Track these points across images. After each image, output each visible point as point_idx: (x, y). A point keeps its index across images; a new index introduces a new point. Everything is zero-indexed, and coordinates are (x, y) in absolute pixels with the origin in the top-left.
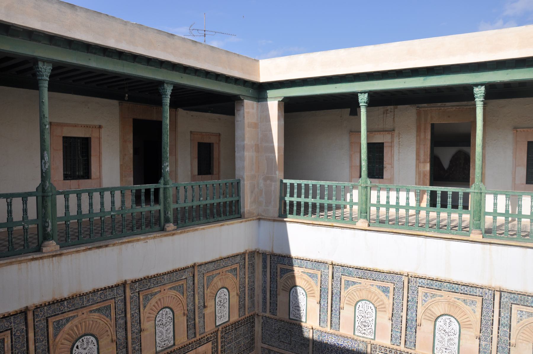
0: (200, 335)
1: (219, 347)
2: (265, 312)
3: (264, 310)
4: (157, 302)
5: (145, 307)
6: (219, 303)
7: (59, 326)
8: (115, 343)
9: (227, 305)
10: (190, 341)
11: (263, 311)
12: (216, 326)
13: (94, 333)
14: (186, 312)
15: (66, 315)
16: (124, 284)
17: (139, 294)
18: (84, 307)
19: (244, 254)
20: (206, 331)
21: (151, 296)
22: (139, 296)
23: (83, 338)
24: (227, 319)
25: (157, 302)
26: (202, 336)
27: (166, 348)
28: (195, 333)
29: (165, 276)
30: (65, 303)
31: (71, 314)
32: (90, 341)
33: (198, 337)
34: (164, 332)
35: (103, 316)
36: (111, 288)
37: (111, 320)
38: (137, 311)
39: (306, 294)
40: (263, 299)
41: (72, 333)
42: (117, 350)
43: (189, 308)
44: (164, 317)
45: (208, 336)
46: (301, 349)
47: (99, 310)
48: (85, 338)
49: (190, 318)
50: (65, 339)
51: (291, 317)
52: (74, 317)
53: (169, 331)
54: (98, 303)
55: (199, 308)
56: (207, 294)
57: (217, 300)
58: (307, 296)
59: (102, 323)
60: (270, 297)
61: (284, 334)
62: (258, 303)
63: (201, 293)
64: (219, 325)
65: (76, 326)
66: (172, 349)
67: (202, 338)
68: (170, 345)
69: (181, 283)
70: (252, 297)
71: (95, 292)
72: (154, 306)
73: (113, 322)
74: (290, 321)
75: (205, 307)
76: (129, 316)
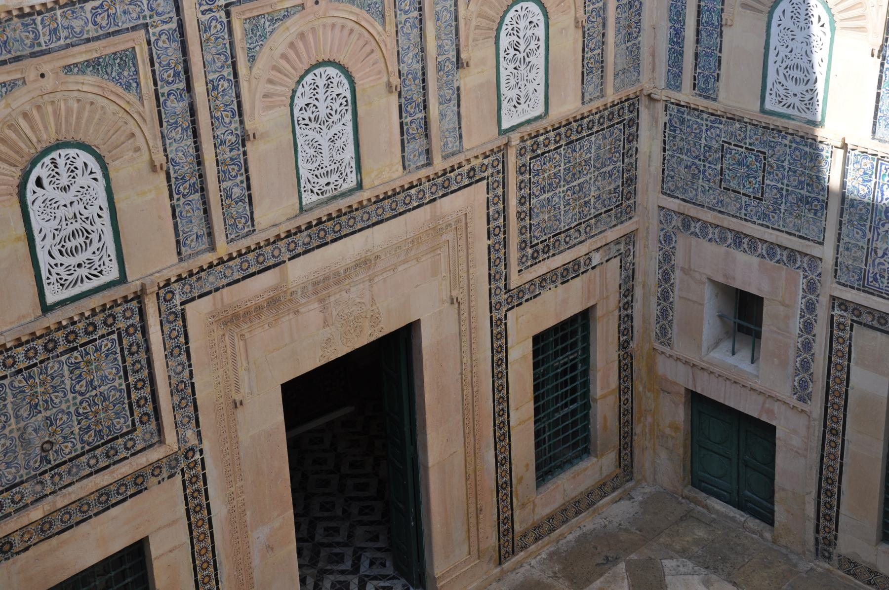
0: (445, 158)
1: (513, 202)
2: (678, 88)
3: (674, 79)
5: (252, 59)
6: (512, 52)
8: (163, 176)
9: (539, 60)
10: (414, 178)
11: (669, 86)
12: (502, 132)
13: (88, 141)
14: (395, 81)
17: (228, 14)
18: (43, 53)
20: (466, 144)
21: (273, 21)
22: (229, 22)
23: (54, 155)
24: (540, 110)
25: (292, 45)
26: (454, 161)
27: (334, 198)
28: (428, 152)
32: (79, 163)
33: (439, 165)
34: (325, 145)
35: (111, 85)
37: (141, 99)
38: (227, 72)
39: (832, 22)
40: (671, 41)
41: (13, 136)
42: (171, 197)
43: (405, 69)
44: (321, 96)
45: (475, 163)
46: (798, 216)
47: (95, 65)
48: (61, 156)
49: (410, 101)
51: (768, 106)
53: (339, 143)
54: (88, 40)
55: (440, 68)
56: (468, 21)
57: (504, 42)
58: (833, 30)
59: (113, 107)
60: (698, 32)
61: (741, 164)
62: (653, 55)
63: (447, 16)
64: (513, 129)
65: (25, 115)
66: (353, 200)
67: (453, 170)
68: (346, 187)
70: (631, 33)
72: (284, 56)
74: (765, 119)
75: (459, 63)
76: (199, 87)
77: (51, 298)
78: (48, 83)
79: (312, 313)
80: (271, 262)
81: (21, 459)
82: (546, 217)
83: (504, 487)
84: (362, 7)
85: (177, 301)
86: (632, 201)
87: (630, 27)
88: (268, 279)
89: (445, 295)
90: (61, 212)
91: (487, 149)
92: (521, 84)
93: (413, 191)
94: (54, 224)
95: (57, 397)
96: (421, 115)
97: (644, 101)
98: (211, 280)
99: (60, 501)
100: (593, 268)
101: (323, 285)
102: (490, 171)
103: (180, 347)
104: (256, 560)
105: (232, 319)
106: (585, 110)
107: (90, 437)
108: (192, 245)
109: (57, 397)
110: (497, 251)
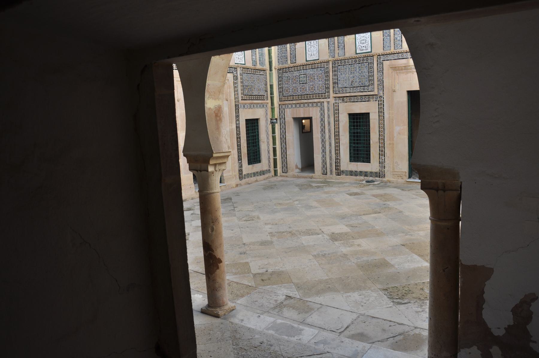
77: (357, 52)
85: (382, 60)
98: (390, 57)
99: (353, 94)
103: (381, 71)
104: (395, 135)
105: (395, 68)
108: (386, 48)
109: (355, 72)
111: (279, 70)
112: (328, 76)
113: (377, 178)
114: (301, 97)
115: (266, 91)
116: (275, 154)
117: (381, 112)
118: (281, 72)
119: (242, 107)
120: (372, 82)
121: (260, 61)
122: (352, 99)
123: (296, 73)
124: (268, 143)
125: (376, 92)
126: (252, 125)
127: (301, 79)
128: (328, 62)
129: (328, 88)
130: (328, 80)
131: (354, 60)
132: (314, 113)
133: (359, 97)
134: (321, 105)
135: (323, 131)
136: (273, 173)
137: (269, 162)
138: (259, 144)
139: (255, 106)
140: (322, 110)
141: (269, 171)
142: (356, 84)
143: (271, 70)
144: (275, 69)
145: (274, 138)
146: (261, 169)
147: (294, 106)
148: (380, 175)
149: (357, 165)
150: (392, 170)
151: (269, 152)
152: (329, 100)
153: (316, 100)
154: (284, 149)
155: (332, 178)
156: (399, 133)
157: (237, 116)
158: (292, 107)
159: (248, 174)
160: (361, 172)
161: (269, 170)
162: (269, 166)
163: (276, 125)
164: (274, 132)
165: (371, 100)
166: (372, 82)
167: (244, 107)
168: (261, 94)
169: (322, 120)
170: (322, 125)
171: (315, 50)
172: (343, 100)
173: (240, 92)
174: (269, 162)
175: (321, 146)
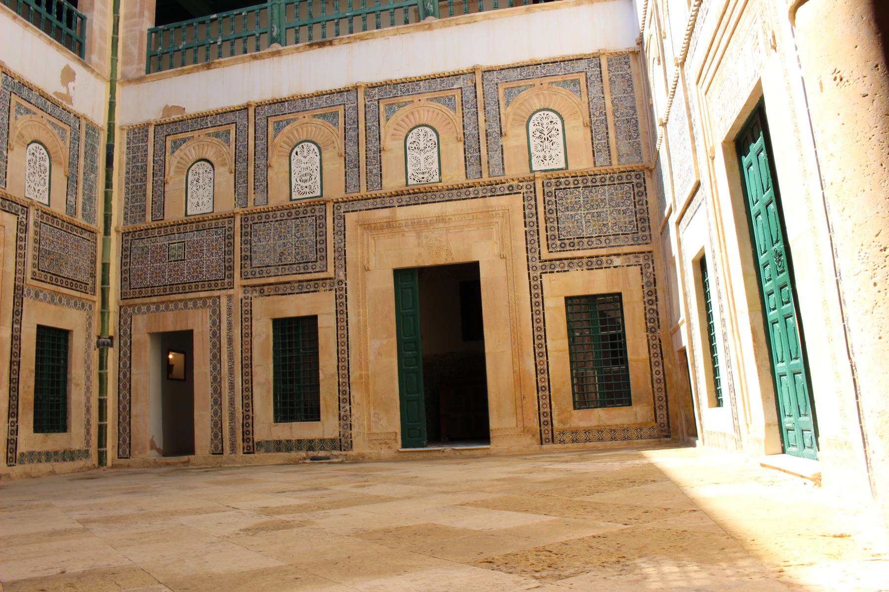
1: (541, 209)
4: (407, 116)
6: (538, 134)
7: (278, 128)
10: (470, 182)
15: (286, 117)
16: (356, 88)
19: (596, 56)
21: (399, 107)
25: (407, 116)
26: (498, 179)
28: (481, 172)
29: (422, 83)
30: (286, 104)
31: (291, 116)
33: (486, 178)
36: (340, 92)
38: (376, 123)
44: (422, 139)
45: (512, 183)
47: (324, 116)
49: (471, 147)
50: (285, 142)
52: (295, 120)
53: (430, 160)
56: (507, 116)
57: (532, 128)
59: (327, 131)
65: (297, 130)
68: (432, 181)
69: (449, 93)
71: (319, 95)
72: (403, 120)
73: (341, 132)
77: (294, 197)
78: (306, 120)
79: (411, 238)
80: (388, 205)
81: (272, 257)
82: (571, 225)
83: (544, 389)
84: (444, 105)
86: (647, 233)
87: (629, 132)
88: (385, 213)
89: (496, 250)
90: (303, 165)
91: (521, 177)
92: (547, 150)
93: (471, 189)
94: (299, 169)
95: (289, 236)
96: (478, 154)
97: (647, 173)
98: (358, 206)
100: (615, 267)
101: (419, 225)
102: (525, 190)
103: (340, 231)
104: (371, 357)
105: (368, 226)
106: (596, 170)
107: (298, 257)
109: (289, 236)
110: (532, 235)
111: (125, 234)
112: (232, 245)
113: (335, 452)
114: (172, 288)
115: (93, 276)
116: (102, 415)
117: (341, 312)
118: (130, 238)
119: (33, 293)
120: (324, 254)
121: (84, 210)
122: (282, 289)
123: (163, 241)
124: (88, 389)
125: (330, 272)
126: (54, 342)
127: (172, 252)
128: (232, 217)
129: (231, 268)
130: (232, 252)
131: (286, 212)
132: (198, 323)
133: (296, 285)
134: (214, 303)
135: (216, 358)
136: (94, 459)
137: (88, 432)
138: (65, 389)
139: (64, 301)
140: (216, 314)
141: (86, 454)
142: (290, 259)
143: (107, 232)
144: (117, 231)
145: (102, 380)
146: (67, 447)
147: (153, 308)
148: (341, 444)
149: (291, 428)
150: (366, 431)
151: (88, 410)
152: (231, 292)
153: (203, 294)
154: (125, 402)
155: (234, 461)
156: (379, 354)
157: (17, 314)
158: (148, 309)
159: (31, 453)
160: (299, 441)
161: (87, 452)
162: (88, 443)
163: (110, 350)
164: (102, 365)
165: (321, 288)
166: (324, 254)
167: (37, 295)
168: (79, 278)
169: (216, 334)
170: (214, 345)
171: (206, 194)
172: (262, 292)
173: (30, 260)
174: (88, 432)
175: (210, 390)
